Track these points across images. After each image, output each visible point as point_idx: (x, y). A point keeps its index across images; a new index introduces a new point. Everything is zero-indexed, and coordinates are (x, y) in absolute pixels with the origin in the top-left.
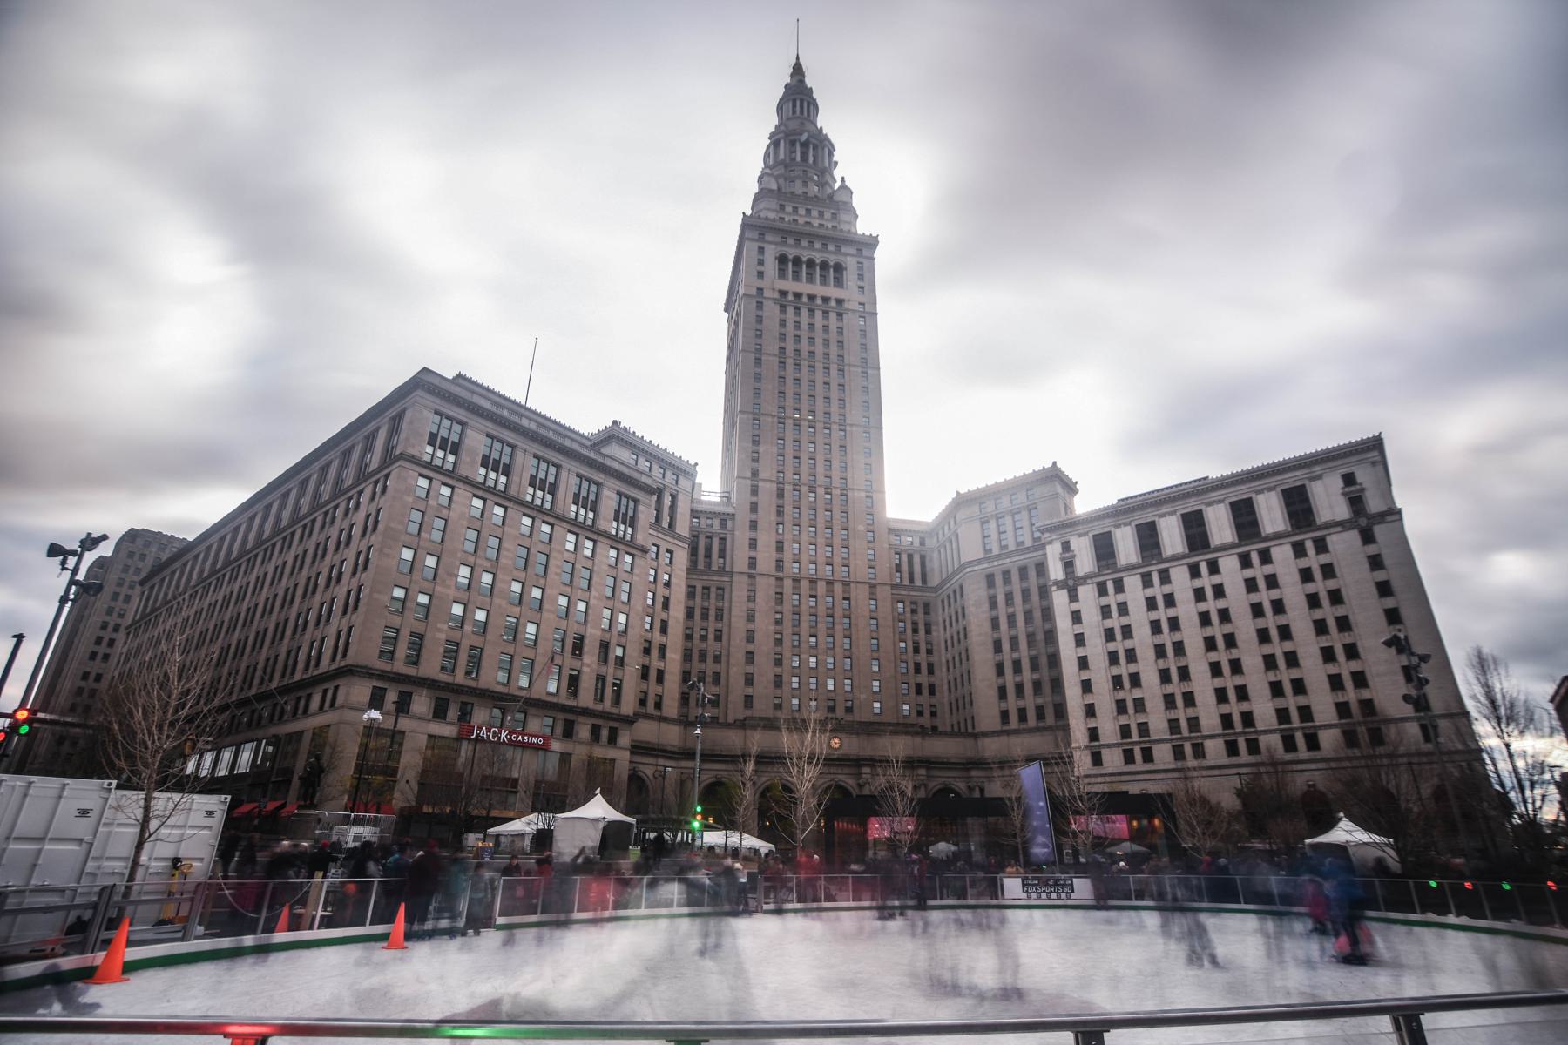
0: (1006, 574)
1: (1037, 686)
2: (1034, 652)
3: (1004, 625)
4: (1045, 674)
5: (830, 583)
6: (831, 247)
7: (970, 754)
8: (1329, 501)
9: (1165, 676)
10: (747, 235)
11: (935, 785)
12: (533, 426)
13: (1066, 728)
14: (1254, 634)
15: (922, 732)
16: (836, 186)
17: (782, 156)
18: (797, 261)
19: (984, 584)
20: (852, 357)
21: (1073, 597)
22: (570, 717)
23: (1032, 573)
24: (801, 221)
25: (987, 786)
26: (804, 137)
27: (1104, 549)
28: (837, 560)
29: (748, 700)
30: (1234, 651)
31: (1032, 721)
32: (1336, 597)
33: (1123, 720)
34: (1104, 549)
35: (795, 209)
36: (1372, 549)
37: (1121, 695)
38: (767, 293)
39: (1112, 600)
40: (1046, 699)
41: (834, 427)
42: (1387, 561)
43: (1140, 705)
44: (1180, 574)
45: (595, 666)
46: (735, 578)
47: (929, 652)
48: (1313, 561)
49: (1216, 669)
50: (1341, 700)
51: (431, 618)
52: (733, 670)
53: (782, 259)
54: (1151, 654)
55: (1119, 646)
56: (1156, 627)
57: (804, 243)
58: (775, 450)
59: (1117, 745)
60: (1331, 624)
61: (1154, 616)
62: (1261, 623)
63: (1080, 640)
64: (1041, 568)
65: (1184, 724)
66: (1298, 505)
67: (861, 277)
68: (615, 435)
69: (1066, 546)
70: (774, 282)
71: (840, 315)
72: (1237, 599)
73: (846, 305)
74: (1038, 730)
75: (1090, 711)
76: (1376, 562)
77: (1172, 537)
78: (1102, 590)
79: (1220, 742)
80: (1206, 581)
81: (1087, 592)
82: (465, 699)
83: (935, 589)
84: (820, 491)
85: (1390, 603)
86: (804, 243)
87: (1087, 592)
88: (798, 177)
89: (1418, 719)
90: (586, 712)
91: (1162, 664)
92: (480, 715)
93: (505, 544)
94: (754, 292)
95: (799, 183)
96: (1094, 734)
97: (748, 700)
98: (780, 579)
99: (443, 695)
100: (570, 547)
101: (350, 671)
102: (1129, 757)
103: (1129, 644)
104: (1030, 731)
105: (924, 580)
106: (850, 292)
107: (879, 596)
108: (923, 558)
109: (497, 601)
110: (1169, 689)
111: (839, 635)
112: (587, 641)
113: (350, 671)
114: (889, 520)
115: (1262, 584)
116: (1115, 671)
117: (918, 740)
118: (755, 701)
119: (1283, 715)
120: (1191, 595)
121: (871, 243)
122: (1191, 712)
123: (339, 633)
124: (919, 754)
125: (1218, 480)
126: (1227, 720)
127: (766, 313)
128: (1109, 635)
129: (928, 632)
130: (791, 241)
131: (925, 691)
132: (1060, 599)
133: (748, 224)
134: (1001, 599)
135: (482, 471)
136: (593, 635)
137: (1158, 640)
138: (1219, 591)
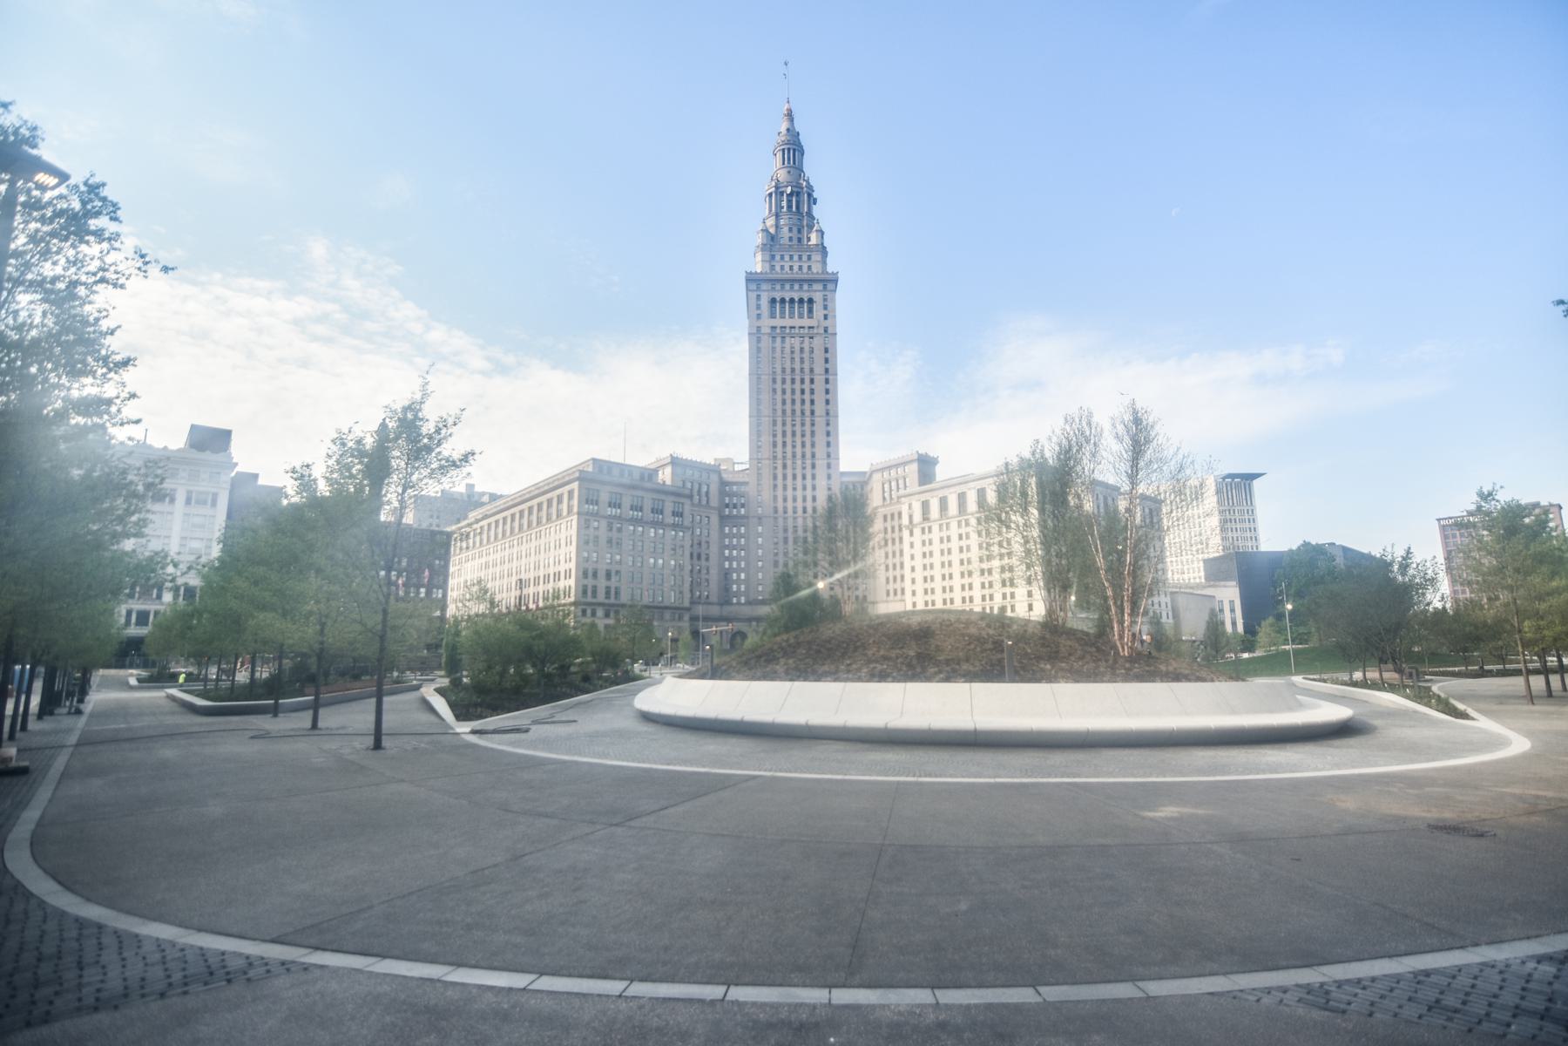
6: (806, 287)
18: (783, 301)
20: (819, 369)
26: (789, 190)
35: (782, 257)
39: (926, 537)
44: (954, 525)
53: (773, 301)
57: (787, 286)
63: (912, 557)
67: (825, 307)
70: (767, 323)
75: (914, 593)
81: (917, 531)
86: (787, 286)
114: (843, 474)
127: (762, 345)
130: (778, 287)
133: (748, 280)
136: (666, 572)
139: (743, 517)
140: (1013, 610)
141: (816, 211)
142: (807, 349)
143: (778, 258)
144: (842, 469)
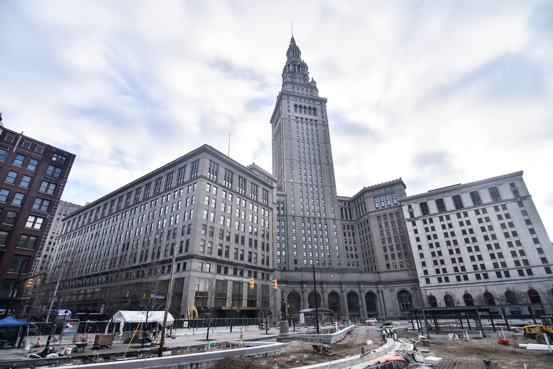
0: (385, 215)
1: (399, 254)
2: (397, 243)
3: (385, 234)
4: (402, 251)
5: (320, 219)
7: (378, 279)
8: (506, 193)
9: (451, 252)
10: (283, 97)
11: (367, 290)
12: (238, 165)
13: (416, 270)
14: (483, 237)
15: (361, 272)
16: (310, 81)
17: (291, 70)
18: (300, 106)
19: (377, 220)
21: (414, 224)
22: (256, 270)
23: (395, 216)
24: (301, 92)
25: (384, 290)
26: (298, 64)
27: (424, 208)
28: (321, 211)
29: (296, 261)
30: (476, 243)
31: (399, 268)
32: (511, 225)
33: (437, 267)
34: (424, 208)
36: (523, 209)
37: (435, 258)
38: (292, 118)
40: (404, 259)
41: (317, 164)
42: (528, 213)
43: (442, 262)
45: (261, 251)
46: (288, 217)
47: (354, 243)
48: (502, 212)
49: (470, 250)
50: (516, 260)
51: (214, 236)
52: (290, 251)
53: (296, 106)
54: (445, 244)
55: (433, 241)
56: (446, 235)
57: (303, 100)
58: (298, 172)
59: (435, 276)
60: (511, 234)
61: (445, 231)
62: (485, 234)
63: (418, 239)
64: (399, 213)
65: (459, 269)
66: (495, 194)
68: (253, 167)
69: (410, 207)
70: (294, 114)
71: (316, 125)
72: (476, 226)
73: (318, 122)
74: (402, 270)
75: (424, 264)
76: (524, 213)
77: (449, 204)
78: (425, 222)
79: (474, 275)
80: (464, 219)
81: (419, 223)
82: (226, 265)
83: (355, 221)
84: (314, 187)
85: (530, 227)
87: (419, 223)
88: (297, 77)
89: (544, 266)
90: (260, 269)
91: (449, 248)
92: (231, 271)
93: (233, 208)
94: (287, 117)
95: (298, 79)
96: (426, 272)
97: (296, 261)
98: (303, 218)
99: (220, 264)
100: (251, 208)
101: (191, 257)
102: (440, 280)
103: (436, 241)
104: (398, 271)
105: (351, 218)
106: (319, 118)
107: (337, 224)
108: (350, 210)
109: (232, 229)
110: (453, 256)
111: (324, 237)
112: (258, 242)
113: (191, 257)
115: (484, 220)
116: (432, 250)
117: (359, 274)
118: (298, 261)
119: (495, 265)
120: (458, 224)
121: (324, 101)
122: (462, 264)
123: (182, 242)
124: (360, 280)
125: (465, 185)
126: (475, 267)
127: (292, 124)
128: (429, 238)
129: (354, 236)
130: (298, 99)
131: (354, 257)
132: (409, 225)
134: (383, 224)
135: (224, 181)
137: (447, 239)
138: (468, 223)
139: (283, 215)
140: (530, 272)
141: (310, 76)
142: (314, 130)
143: (296, 88)
144: (338, 194)
